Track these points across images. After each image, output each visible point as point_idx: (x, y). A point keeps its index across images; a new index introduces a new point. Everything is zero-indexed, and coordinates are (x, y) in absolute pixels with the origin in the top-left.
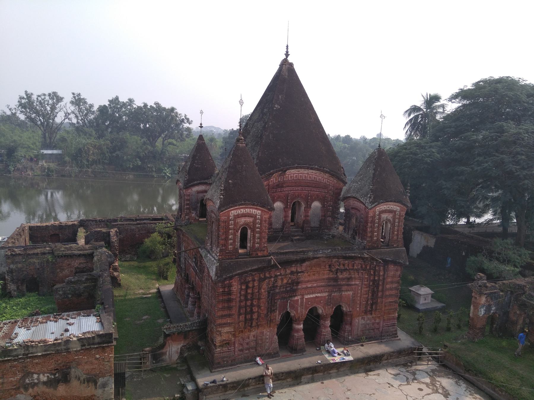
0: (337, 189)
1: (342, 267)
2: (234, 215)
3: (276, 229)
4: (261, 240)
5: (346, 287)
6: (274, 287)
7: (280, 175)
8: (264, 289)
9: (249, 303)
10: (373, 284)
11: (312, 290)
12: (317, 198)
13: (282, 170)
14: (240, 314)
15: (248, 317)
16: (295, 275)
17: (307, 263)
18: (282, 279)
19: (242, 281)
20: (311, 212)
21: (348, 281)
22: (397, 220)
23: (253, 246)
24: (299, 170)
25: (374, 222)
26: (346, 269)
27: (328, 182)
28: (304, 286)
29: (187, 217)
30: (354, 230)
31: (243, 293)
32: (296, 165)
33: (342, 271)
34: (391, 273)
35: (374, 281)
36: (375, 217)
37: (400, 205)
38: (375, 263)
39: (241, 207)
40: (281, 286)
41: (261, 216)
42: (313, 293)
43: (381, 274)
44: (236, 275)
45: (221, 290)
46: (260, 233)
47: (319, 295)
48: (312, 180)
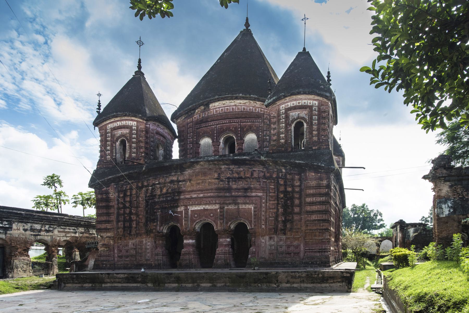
7: (204, 111)
9: (128, 211)
10: (285, 196)
11: (199, 201)
13: (202, 104)
14: (118, 221)
15: (127, 224)
21: (245, 192)
35: (285, 192)
42: (199, 204)
47: (207, 207)
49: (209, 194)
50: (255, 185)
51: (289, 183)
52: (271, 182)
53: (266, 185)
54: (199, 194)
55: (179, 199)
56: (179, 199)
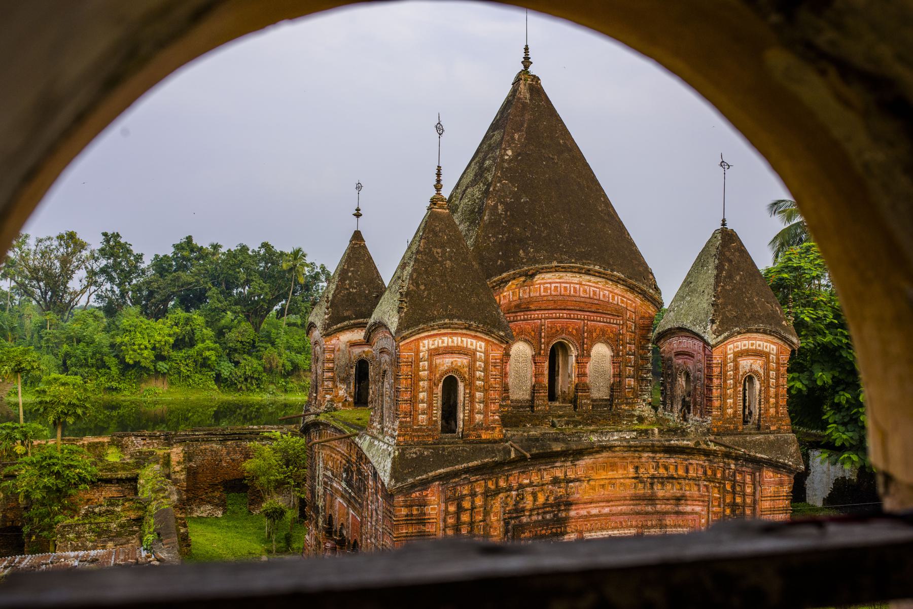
0: (642, 318)
1: (662, 471)
2: (429, 350)
3: (517, 401)
4: (486, 406)
5: (674, 517)
6: (518, 511)
8: (495, 515)
10: (733, 511)
12: (603, 337)
13: (526, 275)
16: (562, 485)
17: (587, 461)
18: (534, 495)
19: (449, 494)
20: (590, 368)
21: (677, 505)
22: (772, 374)
23: (471, 418)
24: (561, 274)
25: (726, 375)
26: (672, 478)
27: (622, 301)
28: (583, 512)
29: (328, 397)
30: (684, 400)
31: (451, 521)
32: (555, 264)
33: (663, 481)
34: (770, 490)
35: (734, 506)
36: (726, 365)
37: (776, 340)
38: (733, 466)
39: (443, 331)
40: (531, 510)
41: (486, 353)
42: (602, 529)
43: (749, 490)
44: (435, 478)
45: (404, 511)
46: (485, 390)
48: (590, 298)
49: (620, 508)
50: (692, 492)
51: (738, 489)
52: (715, 487)
53: (708, 492)
54: (603, 507)
55: (567, 519)
56: (567, 519)
